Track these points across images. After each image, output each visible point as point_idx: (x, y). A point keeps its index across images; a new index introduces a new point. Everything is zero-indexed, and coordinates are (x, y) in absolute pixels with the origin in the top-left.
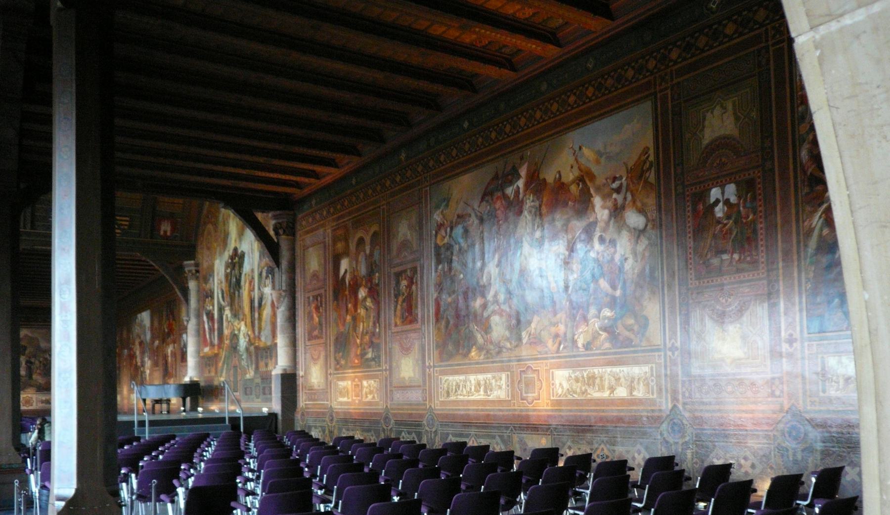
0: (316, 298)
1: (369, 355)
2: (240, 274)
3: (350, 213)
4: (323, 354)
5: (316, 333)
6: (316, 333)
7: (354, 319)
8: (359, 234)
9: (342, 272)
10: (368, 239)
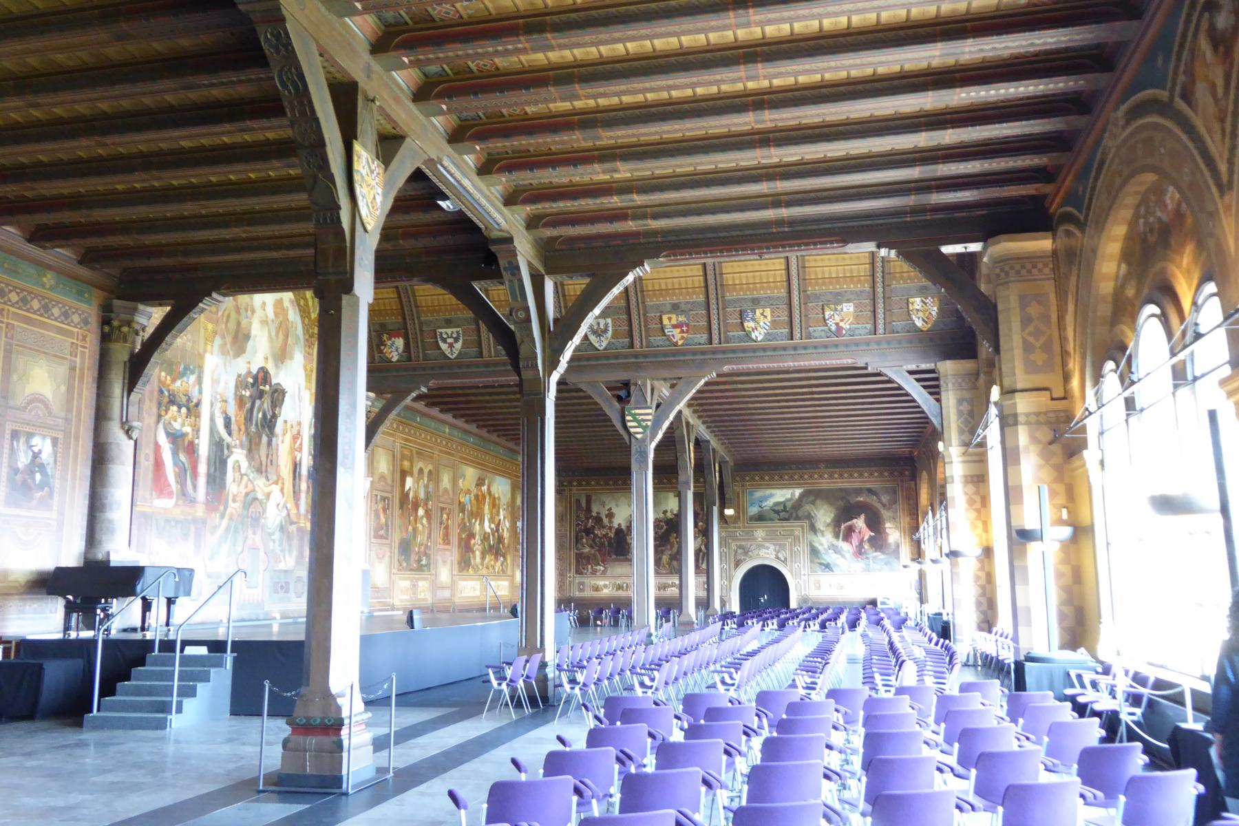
0: (384, 499)
1: (424, 562)
2: (274, 416)
3: (420, 444)
4: (388, 554)
5: (382, 532)
6: (382, 532)
7: (415, 529)
8: (421, 465)
9: (407, 488)
10: (426, 472)
